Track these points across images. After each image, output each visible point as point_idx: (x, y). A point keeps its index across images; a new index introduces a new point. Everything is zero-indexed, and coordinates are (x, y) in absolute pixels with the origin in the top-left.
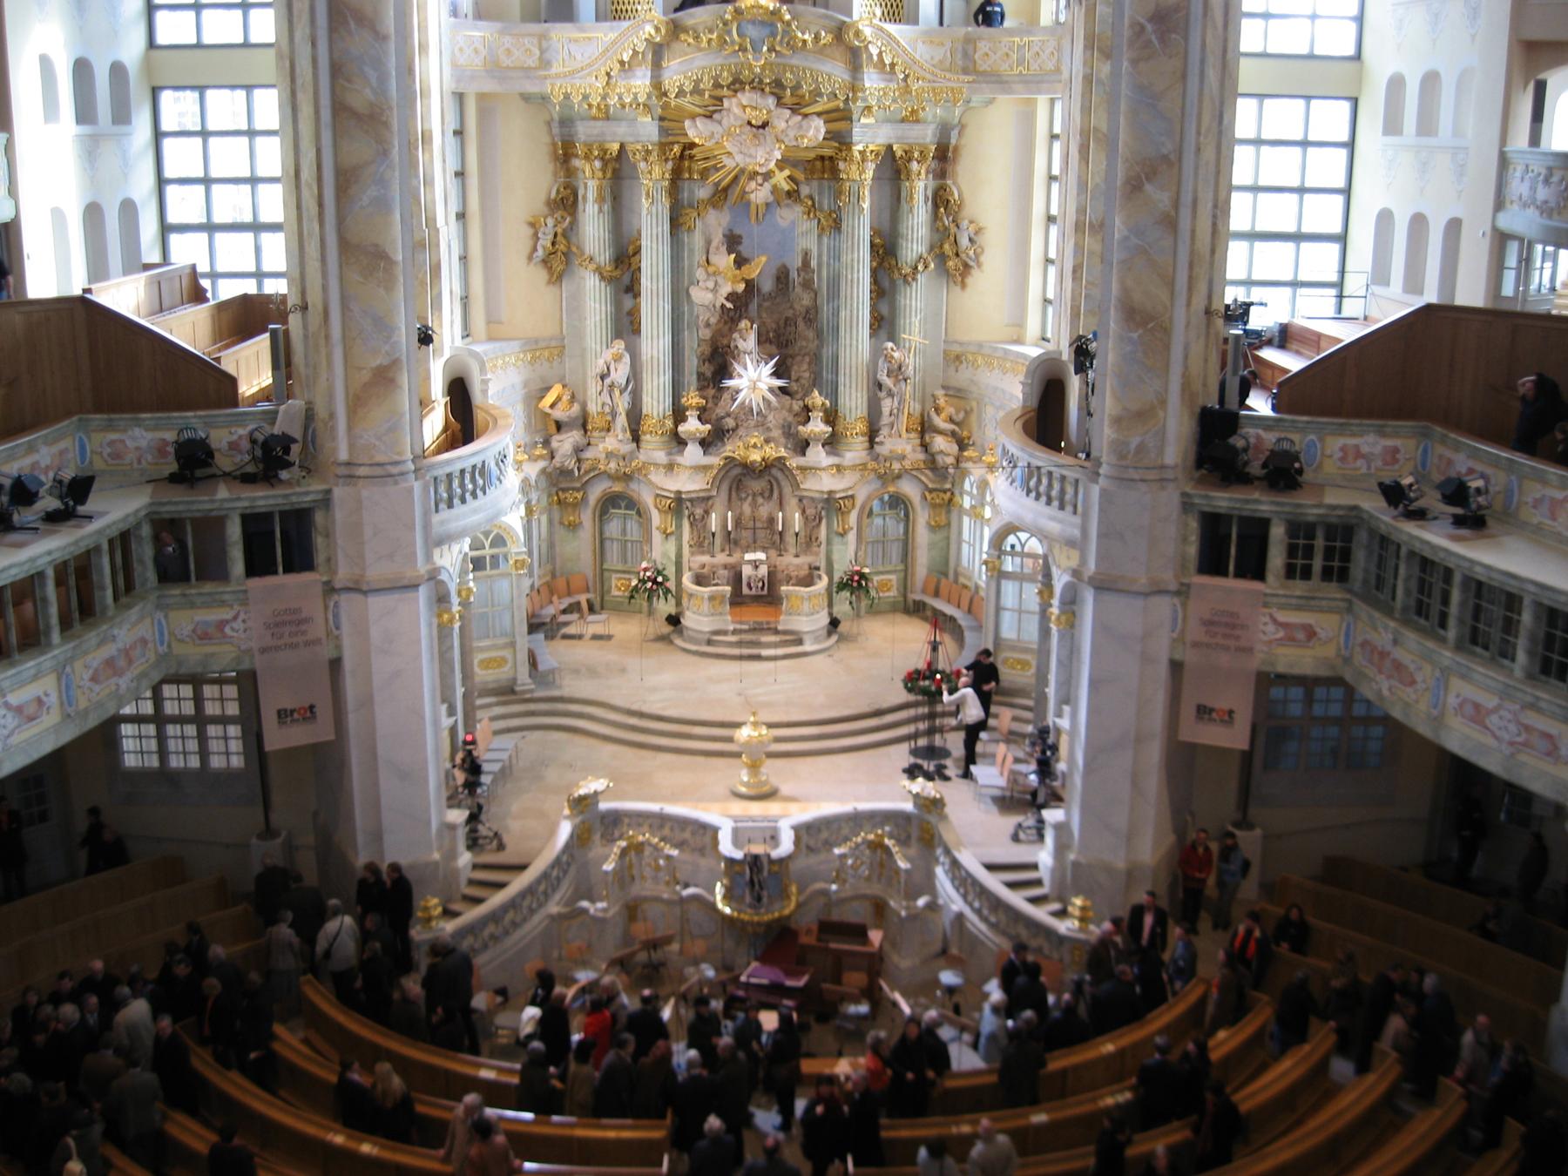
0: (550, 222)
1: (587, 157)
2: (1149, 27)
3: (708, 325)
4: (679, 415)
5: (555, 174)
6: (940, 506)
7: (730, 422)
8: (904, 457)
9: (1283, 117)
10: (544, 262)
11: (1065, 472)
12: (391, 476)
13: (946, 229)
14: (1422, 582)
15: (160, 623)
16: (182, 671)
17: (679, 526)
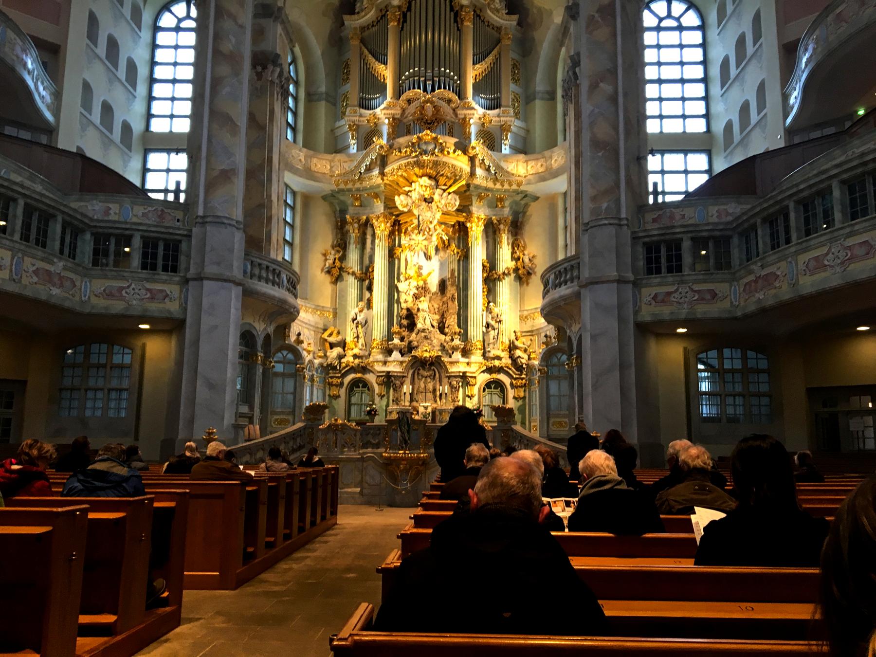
0: (333, 252)
1: (351, 223)
2: (597, 15)
3: (406, 302)
4: (390, 338)
5: (337, 234)
6: (521, 387)
7: (415, 343)
8: (499, 358)
9: (674, 161)
10: (329, 272)
11: (573, 263)
12: (223, 223)
13: (518, 258)
14: (772, 235)
15: (86, 285)
16: (94, 311)
17: (388, 392)
